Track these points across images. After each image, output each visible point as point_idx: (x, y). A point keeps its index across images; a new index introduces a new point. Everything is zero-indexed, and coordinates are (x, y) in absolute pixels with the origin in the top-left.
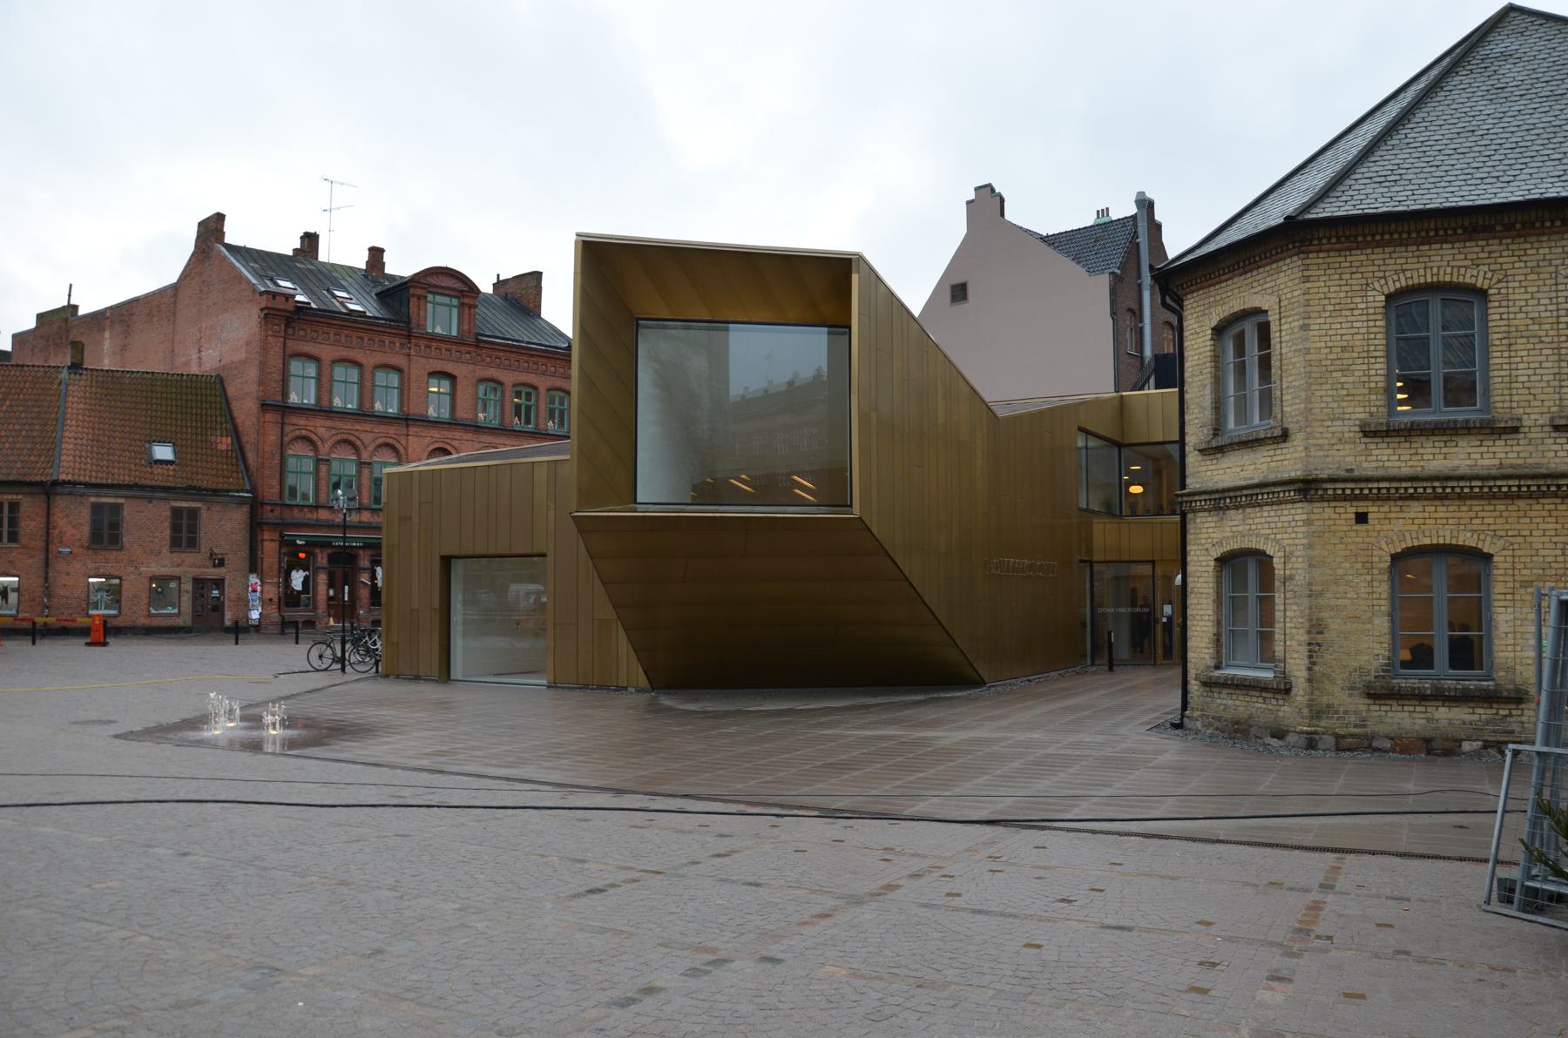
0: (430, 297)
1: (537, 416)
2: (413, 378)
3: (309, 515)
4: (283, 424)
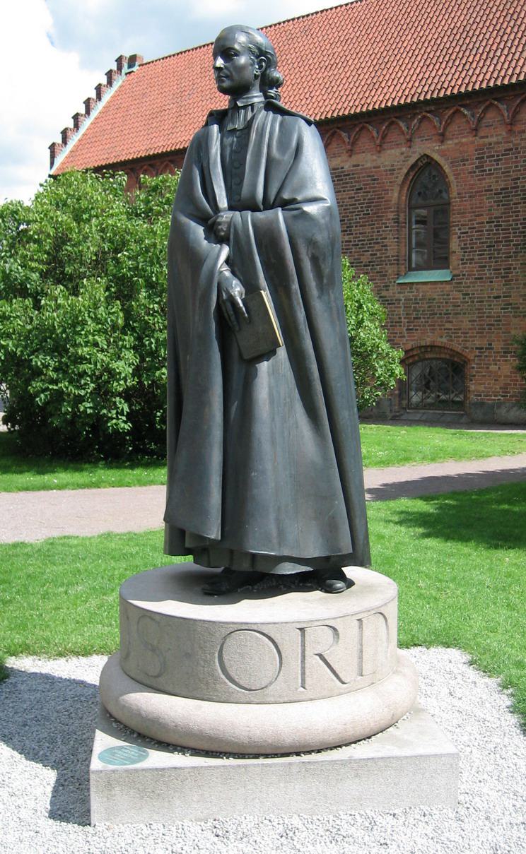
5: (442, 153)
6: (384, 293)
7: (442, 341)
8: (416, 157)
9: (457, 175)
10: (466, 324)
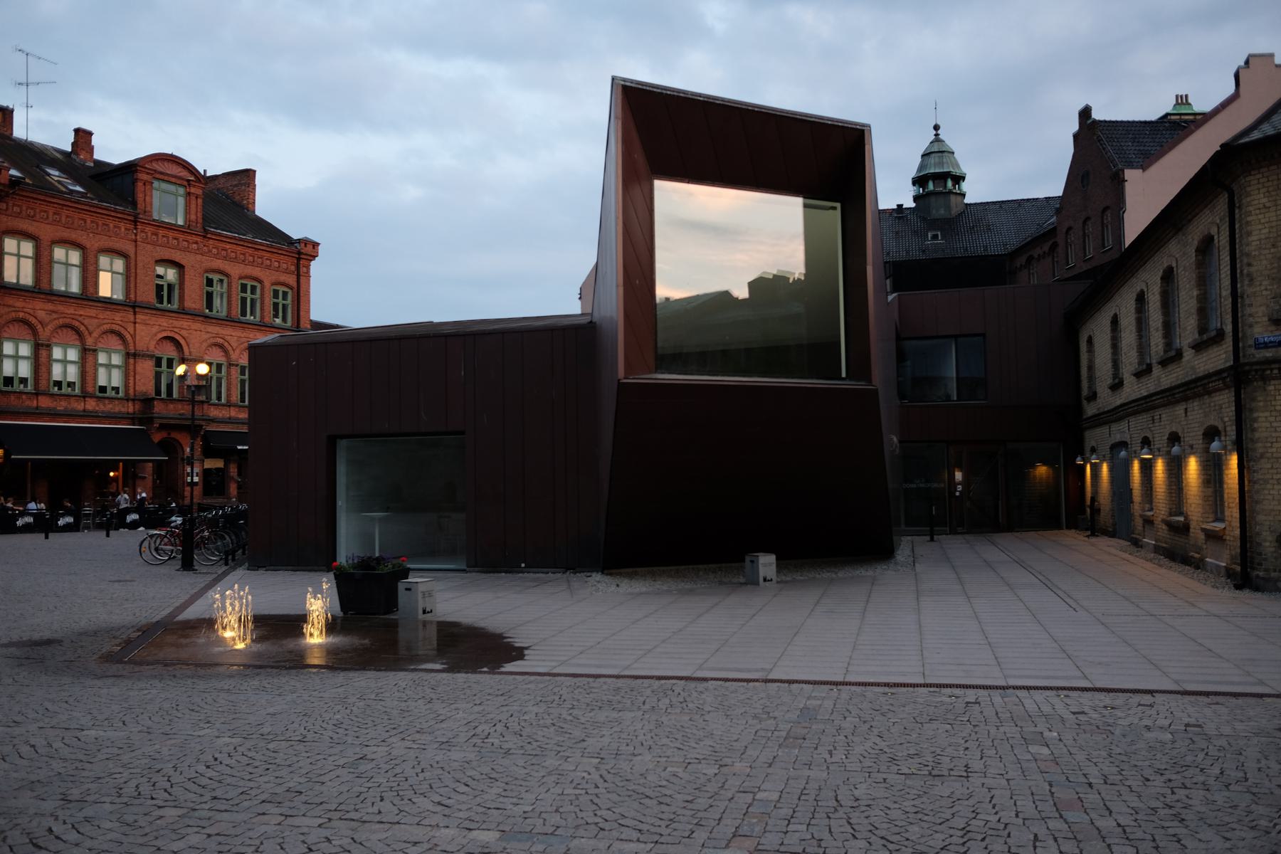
0: (156, 184)
1: (262, 309)
2: (140, 265)
3: (28, 403)
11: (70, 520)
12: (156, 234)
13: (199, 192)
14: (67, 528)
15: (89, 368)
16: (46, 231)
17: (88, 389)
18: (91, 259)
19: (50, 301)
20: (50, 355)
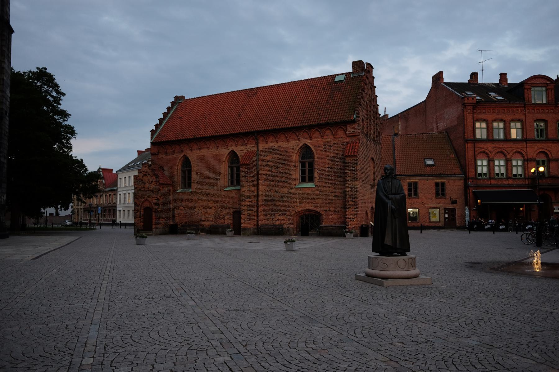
0: (532, 89)
2: (527, 123)
3: (487, 182)
4: (475, 147)
5: (311, 144)
6: (290, 191)
7: (311, 208)
8: (302, 144)
9: (316, 151)
10: (321, 202)
11: (504, 227)
12: (534, 110)
13: (553, 87)
14: (503, 230)
15: (509, 167)
16: (490, 117)
17: (509, 175)
18: (508, 125)
19: (492, 143)
20: (494, 164)
